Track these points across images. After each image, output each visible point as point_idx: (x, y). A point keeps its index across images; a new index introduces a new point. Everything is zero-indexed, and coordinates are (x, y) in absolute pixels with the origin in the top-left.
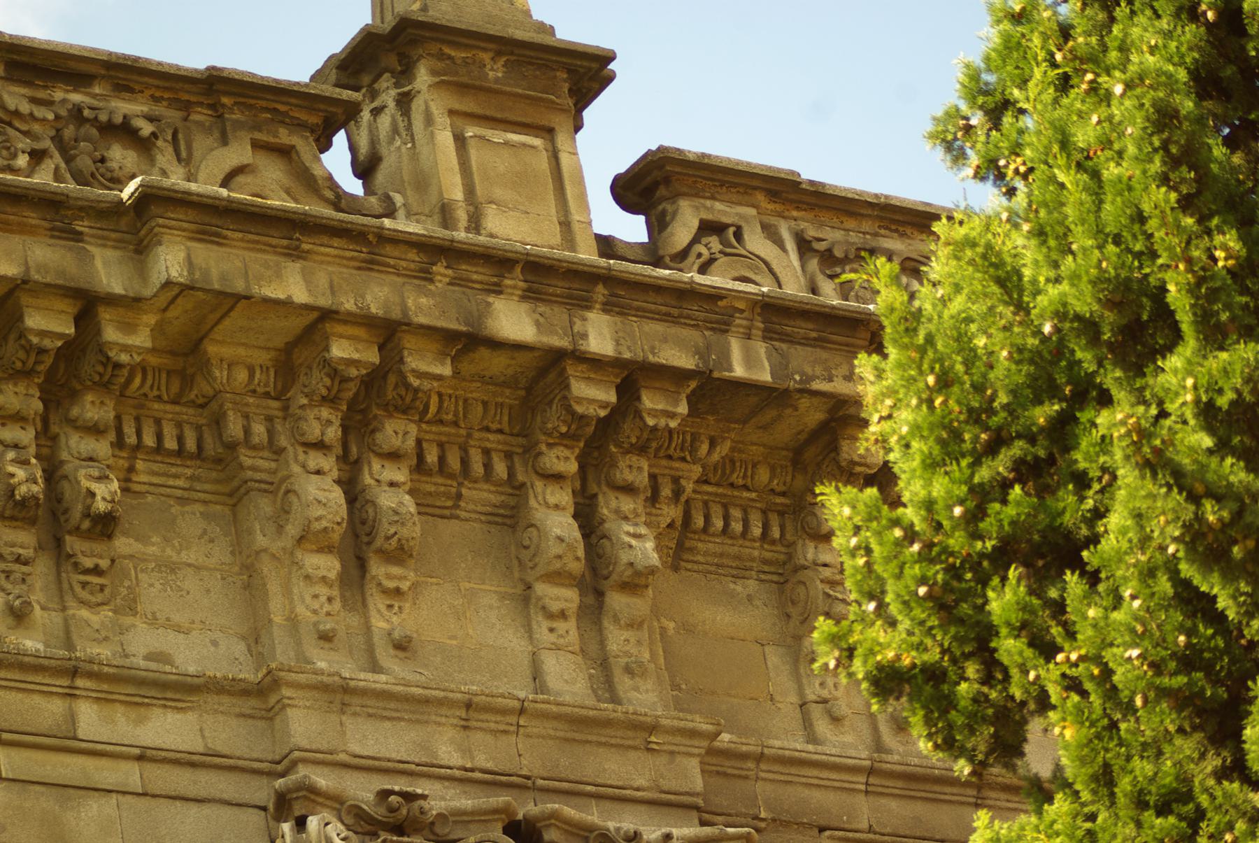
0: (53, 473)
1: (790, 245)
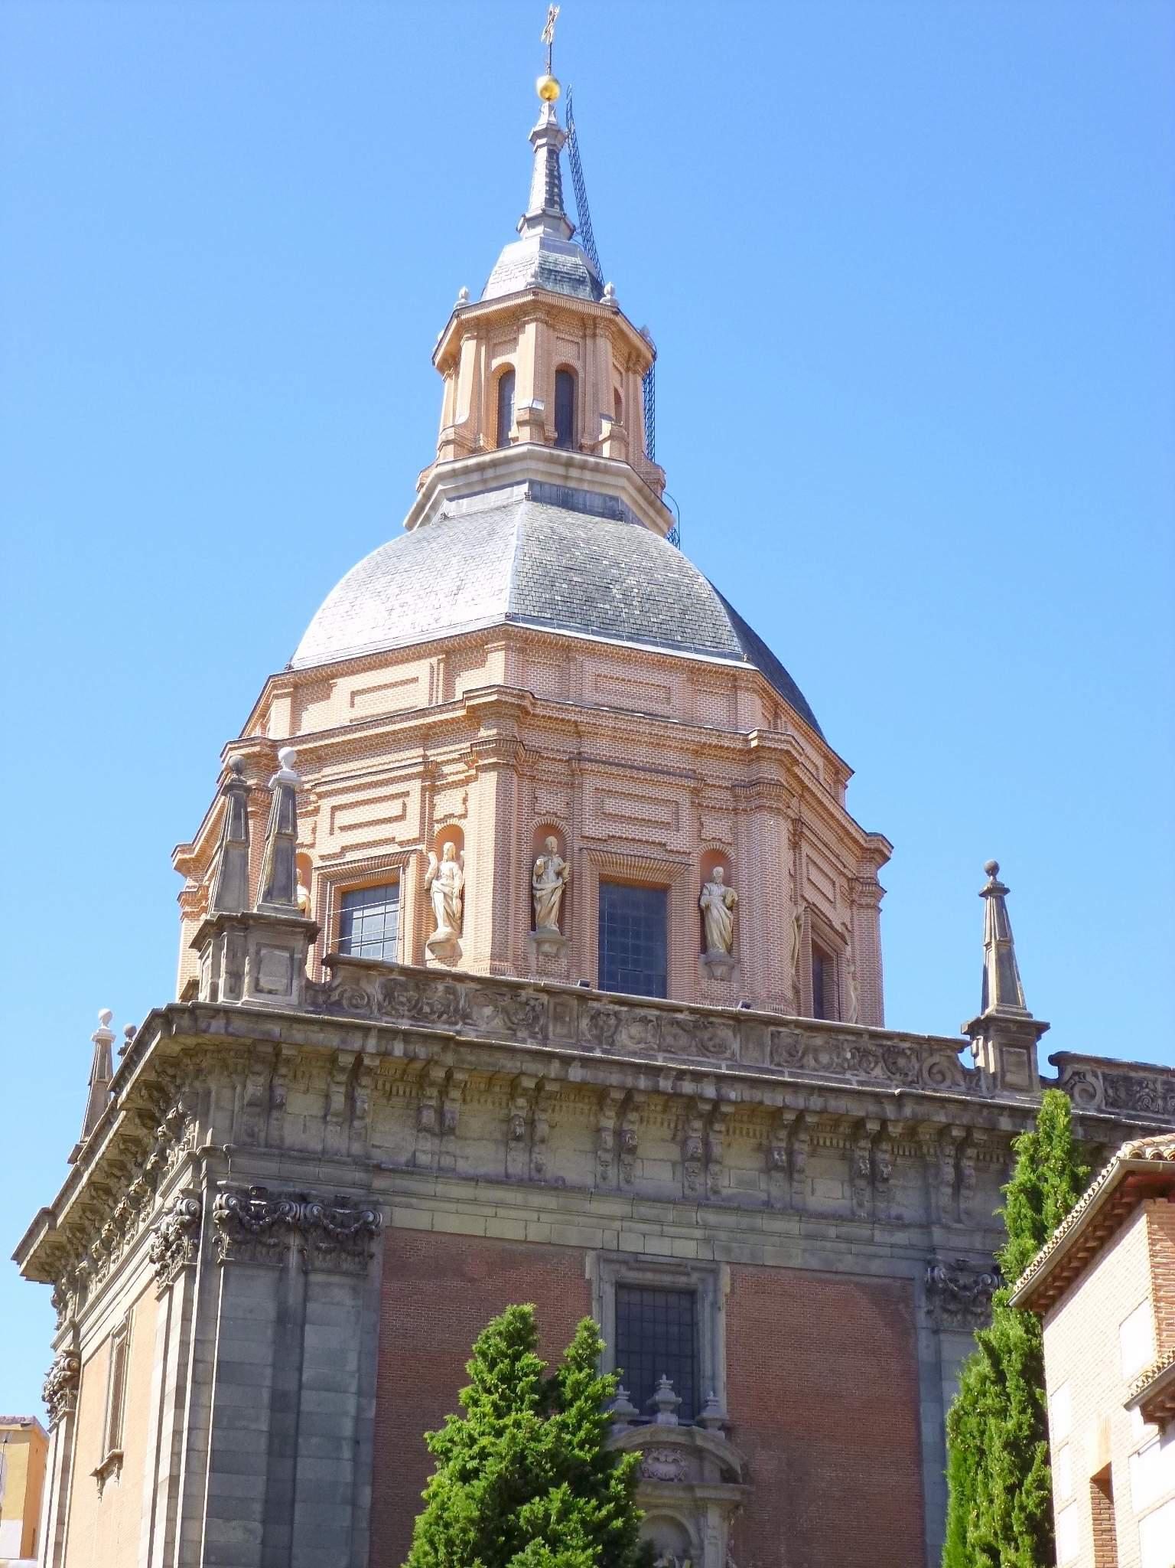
0: (873, 1162)
1: (1100, 1077)
